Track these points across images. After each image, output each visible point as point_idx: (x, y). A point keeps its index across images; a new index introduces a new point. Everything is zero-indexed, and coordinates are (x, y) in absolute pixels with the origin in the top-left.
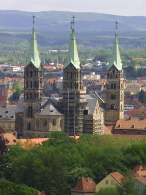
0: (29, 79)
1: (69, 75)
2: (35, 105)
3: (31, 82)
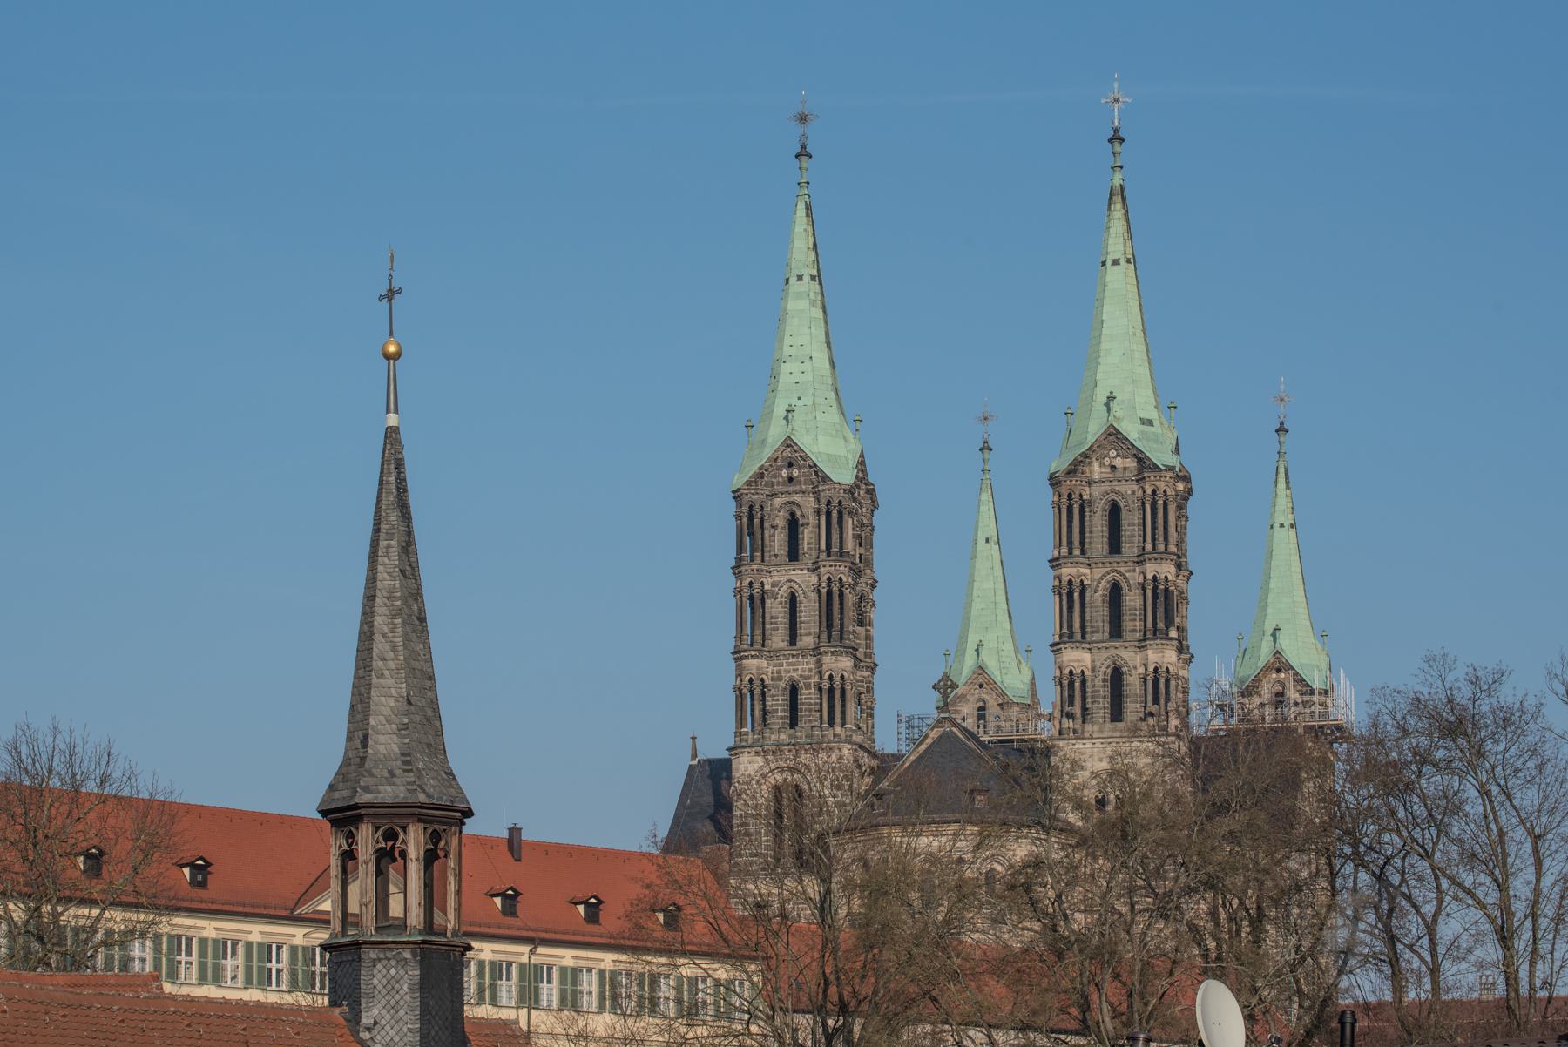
1: (1098, 523)
3: (793, 599)
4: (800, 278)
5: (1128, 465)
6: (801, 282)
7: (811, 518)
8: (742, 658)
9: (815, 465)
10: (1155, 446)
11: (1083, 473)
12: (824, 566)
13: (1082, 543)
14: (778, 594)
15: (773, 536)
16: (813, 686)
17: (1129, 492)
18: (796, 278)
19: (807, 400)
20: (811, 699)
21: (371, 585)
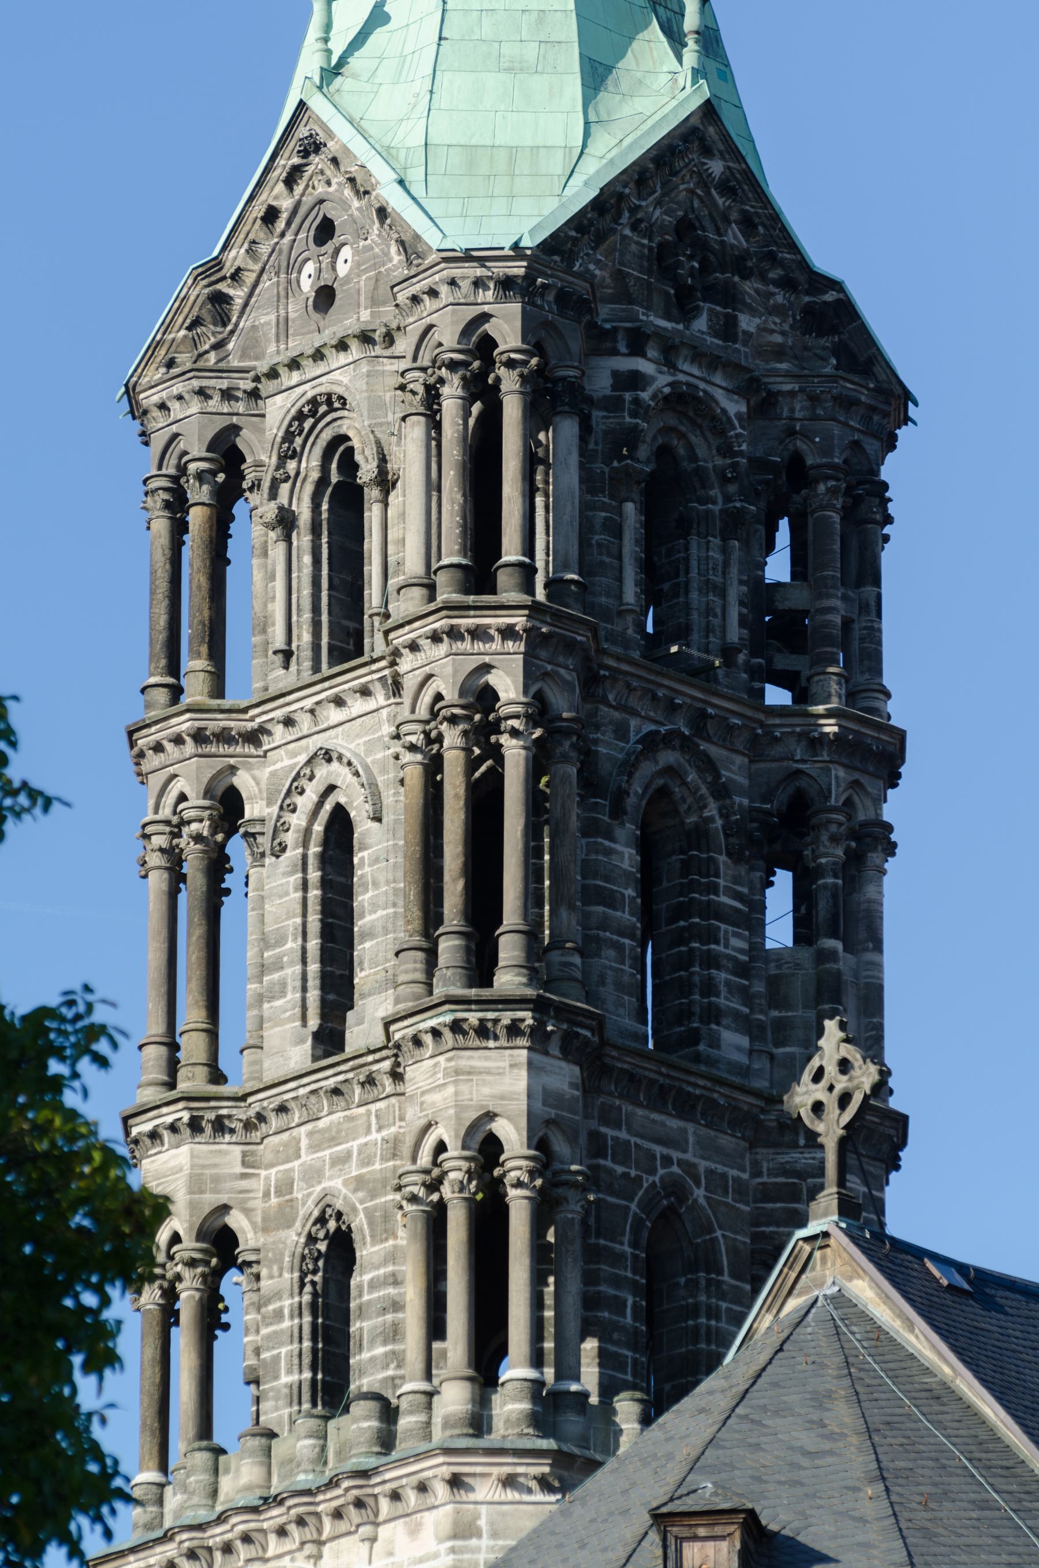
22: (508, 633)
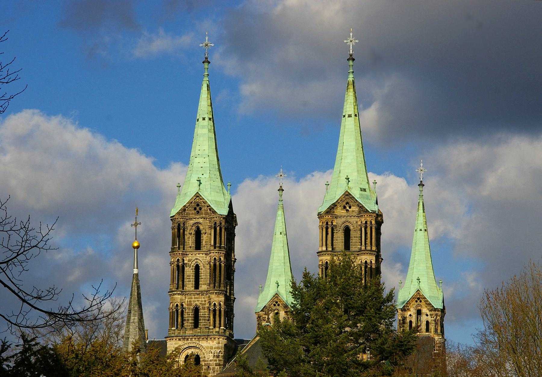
0: (190, 257)
1: (340, 236)
2: (211, 348)
3: (197, 268)
4: (204, 119)
5: (354, 210)
6: (204, 121)
7: (207, 230)
8: (174, 294)
9: (210, 206)
10: (367, 201)
11: (333, 213)
12: (213, 253)
13: (332, 245)
14: (191, 265)
15: (189, 238)
16: (206, 308)
17: (355, 222)
18: (202, 119)
19: (207, 175)
20: (205, 314)
21: (127, 333)
22: (223, 253)
